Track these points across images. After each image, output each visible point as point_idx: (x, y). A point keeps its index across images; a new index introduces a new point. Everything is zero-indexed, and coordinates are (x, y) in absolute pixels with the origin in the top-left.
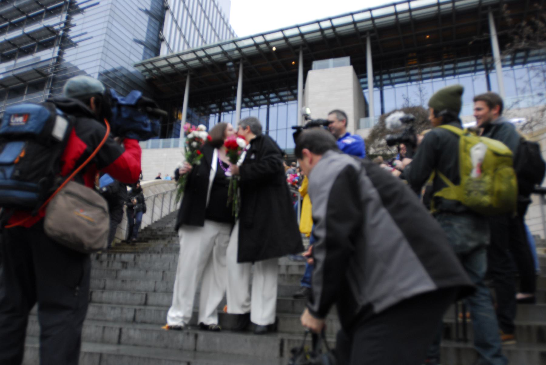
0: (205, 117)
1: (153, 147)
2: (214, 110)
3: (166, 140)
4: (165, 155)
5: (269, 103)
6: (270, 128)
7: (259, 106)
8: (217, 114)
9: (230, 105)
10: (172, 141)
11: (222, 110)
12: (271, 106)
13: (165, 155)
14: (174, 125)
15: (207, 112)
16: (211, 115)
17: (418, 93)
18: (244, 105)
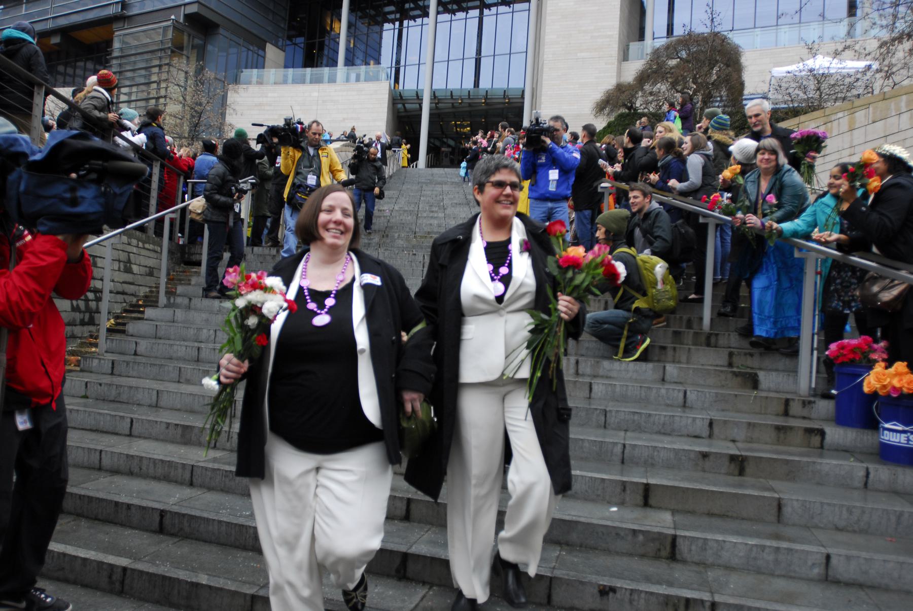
0: (376, 28)
1: (295, 81)
2: (392, 17)
3: (316, 70)
4: (316, 94)
5: (484, 6)
6: (483, 54)
7: (466, 10)
8: (397, 24)
9: (417, 7)
10: (326, 70)
11: (404, 15)
12: (486, 12)
13: (316, 94)
14: (327, 43)
15: (379, 19)
16: (387, 26)
17: (709, 24)
18: (441, 9)
